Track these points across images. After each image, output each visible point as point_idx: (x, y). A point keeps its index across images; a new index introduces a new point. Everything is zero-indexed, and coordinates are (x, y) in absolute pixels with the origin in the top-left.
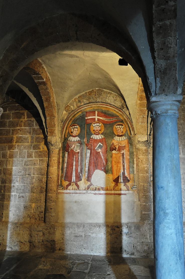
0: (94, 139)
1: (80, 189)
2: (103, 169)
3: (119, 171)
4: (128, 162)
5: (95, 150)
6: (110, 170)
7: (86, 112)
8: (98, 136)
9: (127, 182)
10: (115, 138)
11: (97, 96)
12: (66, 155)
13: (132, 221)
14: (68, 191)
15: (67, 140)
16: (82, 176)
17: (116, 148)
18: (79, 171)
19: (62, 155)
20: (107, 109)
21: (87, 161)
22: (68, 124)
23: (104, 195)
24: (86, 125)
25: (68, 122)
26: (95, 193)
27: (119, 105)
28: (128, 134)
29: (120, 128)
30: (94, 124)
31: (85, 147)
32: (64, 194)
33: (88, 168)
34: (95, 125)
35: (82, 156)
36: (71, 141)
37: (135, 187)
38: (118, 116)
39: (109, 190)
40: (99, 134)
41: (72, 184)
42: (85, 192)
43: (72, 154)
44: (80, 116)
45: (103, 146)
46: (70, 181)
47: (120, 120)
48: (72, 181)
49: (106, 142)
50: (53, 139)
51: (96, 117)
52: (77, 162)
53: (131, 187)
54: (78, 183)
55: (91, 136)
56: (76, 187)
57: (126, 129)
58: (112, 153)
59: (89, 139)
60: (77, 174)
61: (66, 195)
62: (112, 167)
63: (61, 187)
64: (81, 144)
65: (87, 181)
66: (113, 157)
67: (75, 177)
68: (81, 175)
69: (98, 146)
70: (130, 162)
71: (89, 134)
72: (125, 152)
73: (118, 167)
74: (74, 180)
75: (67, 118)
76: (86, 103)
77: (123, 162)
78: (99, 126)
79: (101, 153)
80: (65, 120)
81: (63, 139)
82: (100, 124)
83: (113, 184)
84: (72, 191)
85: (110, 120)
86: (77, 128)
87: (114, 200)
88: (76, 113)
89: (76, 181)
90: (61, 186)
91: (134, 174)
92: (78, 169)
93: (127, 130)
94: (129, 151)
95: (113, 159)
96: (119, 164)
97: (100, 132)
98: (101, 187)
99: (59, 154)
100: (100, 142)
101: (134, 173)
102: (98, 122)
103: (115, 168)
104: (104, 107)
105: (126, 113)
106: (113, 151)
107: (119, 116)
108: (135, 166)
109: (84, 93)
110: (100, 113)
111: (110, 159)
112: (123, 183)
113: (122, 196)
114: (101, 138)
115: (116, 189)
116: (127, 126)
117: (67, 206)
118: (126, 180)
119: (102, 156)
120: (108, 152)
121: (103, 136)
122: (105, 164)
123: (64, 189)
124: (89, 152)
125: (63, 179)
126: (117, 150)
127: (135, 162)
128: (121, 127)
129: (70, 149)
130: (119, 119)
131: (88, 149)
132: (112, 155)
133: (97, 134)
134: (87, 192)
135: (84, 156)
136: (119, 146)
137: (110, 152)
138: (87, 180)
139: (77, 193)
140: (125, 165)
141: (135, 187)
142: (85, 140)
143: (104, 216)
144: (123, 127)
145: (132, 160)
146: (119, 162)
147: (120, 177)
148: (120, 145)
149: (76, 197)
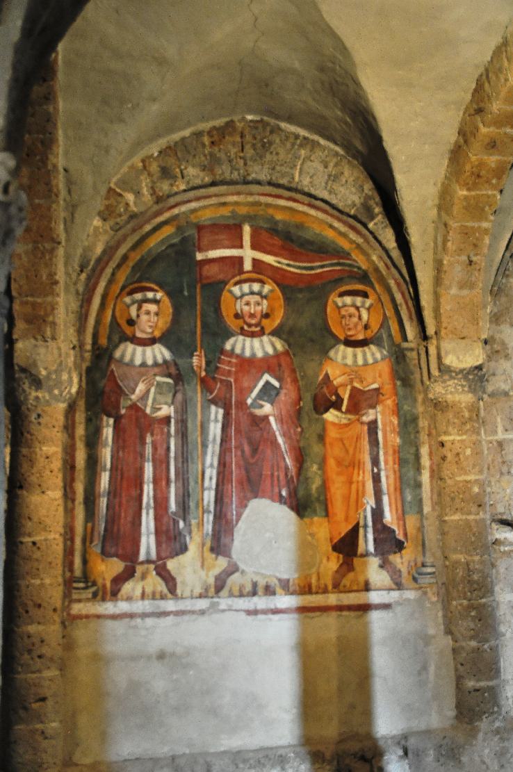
0: (238, 356)
1: (179, 591)
2: (284, 493)
3: (359, 504)
4: (394, 463)
5: (249, 408)
6: (318, 500)
7: (200, 228)
8: (256, 342)
9: (395, 553)
10: (336, 353)
11: (249, 152)
12: (108, 432)
13: (420, 724)
14: (123, 607)
15: (111, 358)
16: (190, 533)
18: (173, 506)
19: (87, 429)
20: (298, 219)
21: (211, 458)
22: (111, 282)
23: (295, 616)
24: (198, 290)
25: (109, 271)
26: (251, 607)
27: (349, 202)
28: (390, 336)
29: (357, 308)
30: (236, 284)
31: (199, 395)
32: (101, 621)
33: (213, 493)
34: (241, 289)
35: (183, 434)
36: (127, 365)
37: (429, 570)
38: (340, 254)
39: (314, 589)
40: (262, 333)
41: (139, 569)
42: (203, 604)
43: (136, 426)
44: (172, 246)
45: (281, 387)
46: (130, 557)
47: (356, 270)
48: (142, 557)
49: (293, 371)
50: (42, 351)
51: (248, 254)
52: (161, 463)
53: (409, 572)
54: (171, 565)
55: (224, 343)
56: (161, 587)
57: (385, 314)
58: (324, 422)
59: (216, 354)
60: (165, 520)
61: (118, 627)
62: (325, 487)
63: (86, 588)
64: (179, 378)
65: (214, 556)
66: (328, 440)
67: (152, 538)
68: (181, 524)
69: (261, 391)
70: (402, 462)
71: (217, 332)
73: (354, 487)
74: (148, 553)
75: (104, 252)
76: (198, 182)
78: (259, 294)
79: (272, 419)
80: (99, 260)
81: (88, 355)
82: (267, 288)
83: (332, 564)
84: (139, 606)
87: (338, 638)
88: (148, 228)
92: (167, 499)
93: (385, 317)
94: (398, 411)
95: (328, 446)
96: (356, 471)
98: (280, 580)
99: (69, 428)
100: (270, 370)
101: (420, 511)
102: (254, 276)
103: (337, 490)
104: (282, 209)
105: (384, 242)
106: (327, 410)
107: (349, 254)
108: (425, 477)
109: (187, 133)
110: (264, 235)
111: (316, 448)
112: (376, 555)
113: (375, 616)
114: (270, 351)
115: (345, 586)
116: (385, 298)
117: (119, 677)
118: (389, 543)
119: (277, 433)
121: (280, 345)
123: (99, 597)
124: (216, 417)
125: (96, 548)
126: (344, 408)
127: (426, 461)
128: (359, 304)
129: (124, 403)
130: (350, 265)
131: (214, 402)
132: (324, 429)
133: (253, 335)
134: (214, 606)
135: (195, 435)
136: (354, 389)
137: (317, 416)
138: (212, 550)
139: (165, 614)
140: (383, 474)
141: (430, 574)
142: (198, 361)
143: (295, 711)
144: (367, 305)
145: (413, 450)
146: (355, 464)
147: (361, 531)
148: (357, 385)
149: (161, 634)
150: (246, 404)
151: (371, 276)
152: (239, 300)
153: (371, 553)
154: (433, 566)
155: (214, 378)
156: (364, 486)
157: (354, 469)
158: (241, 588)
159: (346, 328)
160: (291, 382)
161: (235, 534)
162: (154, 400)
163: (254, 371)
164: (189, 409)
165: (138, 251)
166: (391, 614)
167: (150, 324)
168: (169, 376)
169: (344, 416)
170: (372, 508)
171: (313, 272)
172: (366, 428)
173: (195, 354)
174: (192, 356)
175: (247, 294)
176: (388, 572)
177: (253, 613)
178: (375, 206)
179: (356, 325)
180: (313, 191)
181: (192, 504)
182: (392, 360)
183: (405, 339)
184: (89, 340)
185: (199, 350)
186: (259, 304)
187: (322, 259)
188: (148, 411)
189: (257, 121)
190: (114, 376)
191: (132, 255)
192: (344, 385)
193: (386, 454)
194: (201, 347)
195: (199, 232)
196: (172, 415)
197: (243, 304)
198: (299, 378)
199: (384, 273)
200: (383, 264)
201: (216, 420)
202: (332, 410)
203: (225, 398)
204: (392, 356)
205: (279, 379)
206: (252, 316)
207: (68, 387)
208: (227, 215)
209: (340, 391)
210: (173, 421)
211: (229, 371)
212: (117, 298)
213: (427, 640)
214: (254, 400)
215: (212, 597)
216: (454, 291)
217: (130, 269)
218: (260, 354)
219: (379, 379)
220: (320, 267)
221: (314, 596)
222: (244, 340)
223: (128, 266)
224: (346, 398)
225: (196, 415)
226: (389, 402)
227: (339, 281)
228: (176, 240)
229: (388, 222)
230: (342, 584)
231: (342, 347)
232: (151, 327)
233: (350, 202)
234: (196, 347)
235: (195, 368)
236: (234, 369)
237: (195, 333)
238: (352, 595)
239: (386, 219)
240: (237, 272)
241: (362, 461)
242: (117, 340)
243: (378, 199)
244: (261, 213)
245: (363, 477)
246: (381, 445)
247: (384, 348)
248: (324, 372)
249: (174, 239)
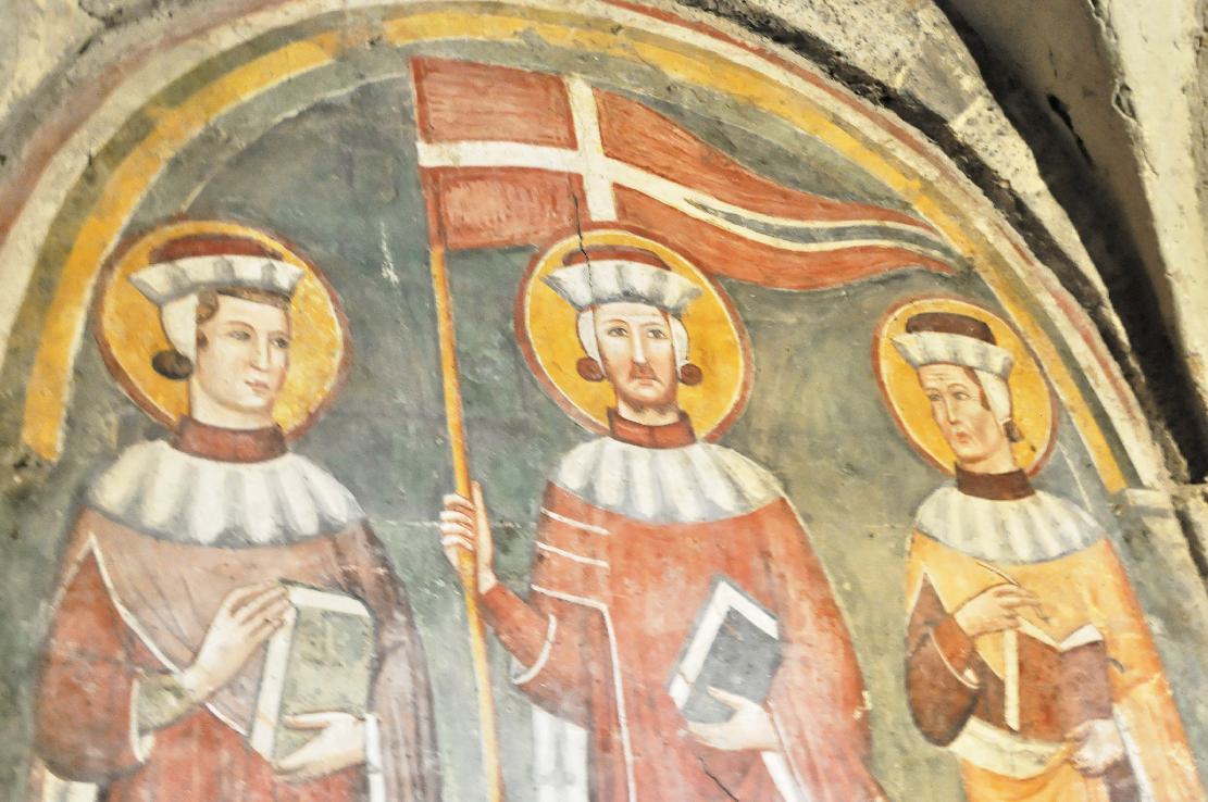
0: (610, 516)
7: (422, 69)
15: (81, 503)
17: (992, 684)
20: (729, 87)
22: (80, 203)
24: (435, 269)
25: (70, 164)
30: (570, 259)
31: (480, 665)
34: (590, 280)
36: (158, 536)
40: (682, 433)
44: (325, 109)
47: (936, 254)
49: (814, 574)
51: (602, 178)
55: (553, 464)
58: (962, 770)
59: (526, 513)
64: (388, 596)
71: (521, 425)
75: (50, 88)
79: (773, 763)
85: (808, 237)
86: (277, 296)
88: (227, 38)
97: (706, 408)
106: (957, 725)
110: (643, 120)
114: (727, 503)
121: (757, 485)
124: (559, 762)
126: (1012, 717)
128: (972, 361)
129: (147, 709)
130: (917, 239)
131: (538, 695)
133: (653, 439)
136: (1025, 642)
137: (933, 750)
148: (1029, 629)
150: (670, 702)
151: (984, 276)
155: (532, 599)
159: (951, 433)
160: (819, 616)
162: (290, 689)
163: (675, 573)
164: (443, 728)
165: (192, 106)
167: (254, 376)
168: (350, 586)
169: (1019, 746)
171: (813, 247)
173: (448, 499)
174: (435, 508)
175: (612, 300)
178: (958, 71)
179: (980, 430)
182: (1116, 545)
183: (1133, 478)
186: (657, 334)
187: (830, 212)
188: (262, 742)
190: (99, 585)
191: (169, 120)
194: (470, 478)
195: (418, 79)
196: (374, 757)
197: (603, 328)
198: (839, 601)
199: (1019, 272)
200: (1011, 248)
201: (562, 776)
202: (974, 724)
203: (587, 680)
204: (1110, 531)
205: (773, 606)
206: (641, 371)
208: (507, 40)
209: (986, 652)
211: (588, 571)
212: (109, 266)
214: (698, 686)
217: (162, 167)
219: (1093, 610)
220: (824, 236)
223: (154, 158)
224: (1010, 675)
225: (479, 757)
226: (1146, 693)
228: (338, 94)
229: (1004, 120)
231: (953, 496)
232: (259, 387)
233: (887, 55)
234: (449, 472)
235: (452, 555)
237: (442, 419)
239: (998, 112)
240: (567, 222)
242: (112, 436)
243: (963, 53)
244: (618, 52)
248: (919, 584)
249: (330, 87)
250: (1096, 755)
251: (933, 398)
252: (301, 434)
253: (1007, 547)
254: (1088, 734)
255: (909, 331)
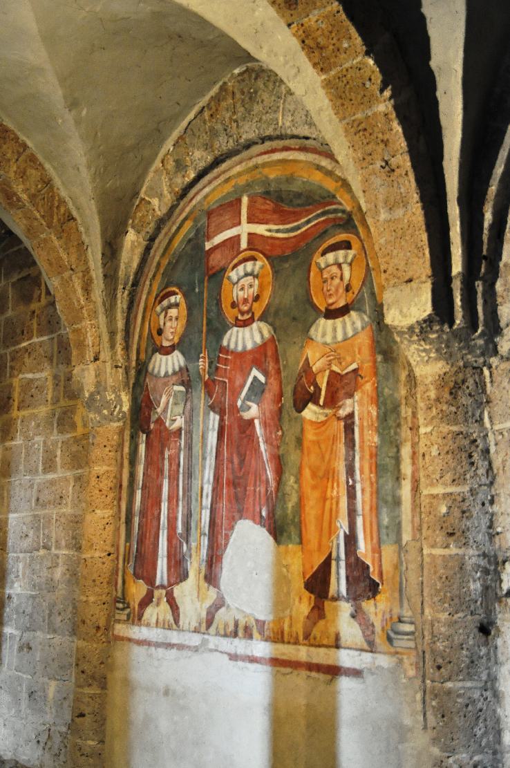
0: (232, 352)
2: (264, 514)
3: (332, 530)
4: (371, 472)
6: (293, 521)
7: (209, 214)
9: (369, 598)
10: (316, 330)
15: (147, 371)
16: (190, 557)
17: (318, 389)
18: (180, 529)
21: (209, 474)
23: (268, 668)
29: (340, 266)
31: (202, 401)
32: (131, 644)
33: (208, 511)
37: (408, 628)
39: (286, 640)
40: (252, 320)
41: (157, 593)
42: (195, 640)
45: (266, 383)
46: (150, 581)
47: (340, 215)
48: (158, 583)
53: (383, 629)
57: (368, 265)
58: (303, 419)
60: (174, 542)
62: (300, 505)
66: (306, 444)
69: (249, 389)
70: (379, 469)
71: (217, 329)
72: (358, 405)
73: (328, 503)
77: (347, 473)
79: (257, 422)
83: (303, 606)
85: (298, 228)
87: (307, 705)
89: (170, 584)
90: (123, 603)
91: (400, 547)
94: (378, 398)
96: (330, 484)
97: (258, 309)
98: (257, 621)
101: (398, 540)
106: (305, 406)
108: (406, 491)
111: (293, 457)
112: (347, 600)
113: (345, 683)
117: (143, 706)
118: (365, 584)
119: (260, 439)
120: (285, 415)
122: (273, 484)
126: (321, 403)
127: (407, 468)
130: (335, 211)
131: (212, 408)
132: (302, 431)
134: (205, 642)
135: (197, 449)
136: (332, 372)
137: (297, 414)
138: (206, 577)
140: (358, 487)
145: (392, 452)
146: (328, 475)
147: (334, 563)
148: (335, 368)
150: (237, 406)
152: (236, 286)
153: (343, 596)
154: (412, 623)
156: (338, 503)
157: (328, 482)
158: (226, 625)
161: (224, 560)
164: (194, 419)
166: (362, 686)
170: (345, 533)
171: (299, 232)
172: (342, 424)
176: (360, 624)
177: (234, 657)
180: (296, 132)
181: (193, 525)
184: (134, 357)
185: (203, 351)
189: (244, 72)
192: (322, 371)
193: (362, 458)
196: (183, 426)
197: (239, 289)
201: (213, 429)
202: (310, 405)
205: (265, 373)
206: (245, 301)
207: (118, 407)
209: (318, 380)
210: (183, 432)
213: (403, 733)
214: (243, 402)
215: (204, 634)
216: (383, 216)
218: (249, 346)
221: (286, 646)
222: (238, 332)
227: (323, 235)
230: (312, 635)
231: (322, 321)
235: (201, 371)
236: (229, 368)
237: (202, 332)
238: (322, 650)
241: (336, 470)
244: (258, 176)
245: (338, 493)
246: (357, 447)
247: (365, 312)
250: (343, 413)
251: (324, 282)
252: (178, 344)
253: (335, 337)
254: (343, 405)
255: (322, 255)
